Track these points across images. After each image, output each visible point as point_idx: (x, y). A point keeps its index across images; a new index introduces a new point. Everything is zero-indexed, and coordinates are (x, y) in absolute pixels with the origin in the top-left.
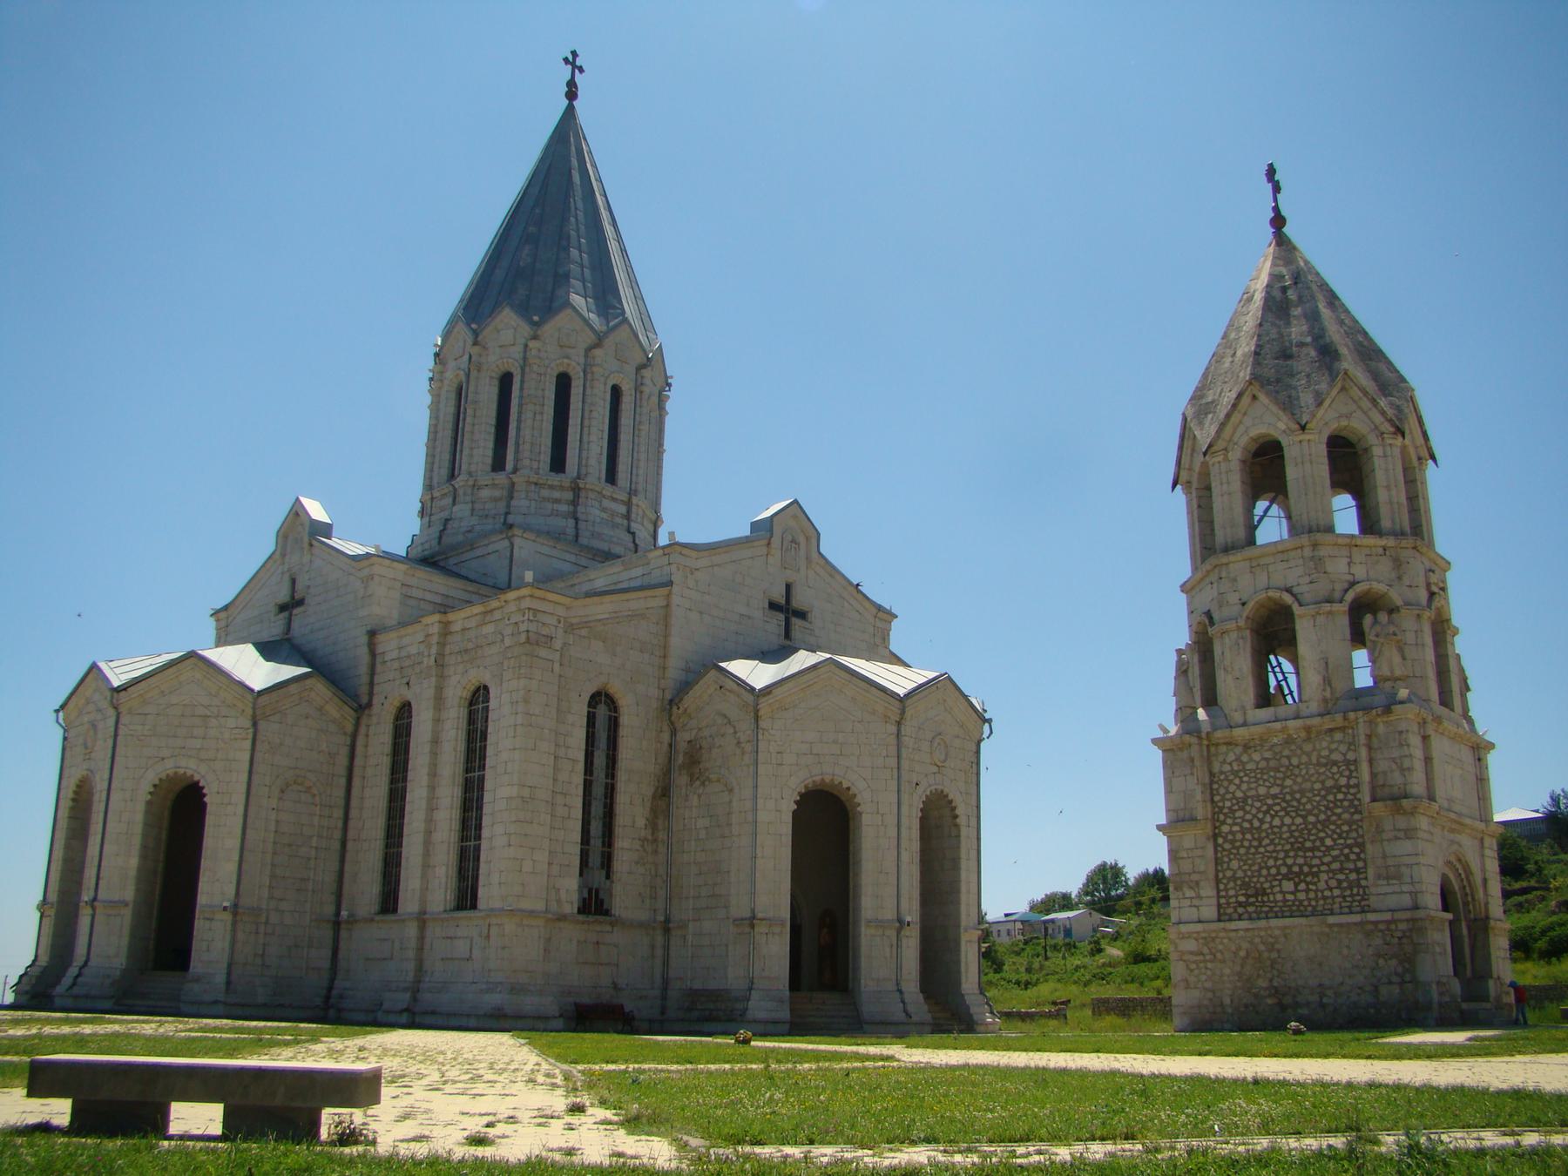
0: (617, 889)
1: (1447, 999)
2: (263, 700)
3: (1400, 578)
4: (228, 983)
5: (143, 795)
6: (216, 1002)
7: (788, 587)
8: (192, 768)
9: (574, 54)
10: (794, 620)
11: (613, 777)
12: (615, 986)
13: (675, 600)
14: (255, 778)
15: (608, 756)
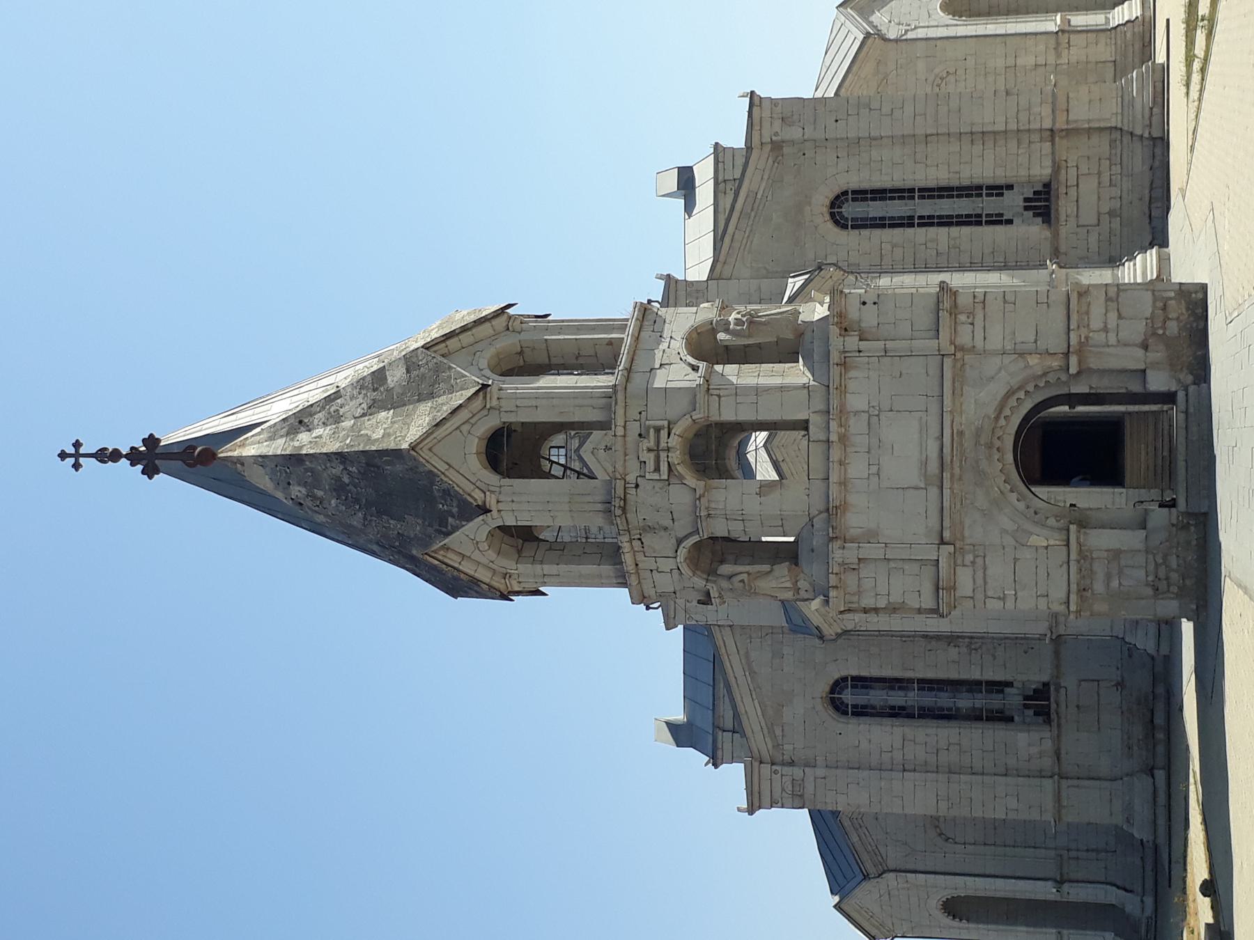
0: (1020, 678)
1: (1173, 562)
2: (872, 871)
3: (666, 529)
4: (1126, 890)
5: (964, 924)
6: (1142, 901)
8: (934, 903)
11: (910, 681)
12: (1120, 685)
14: (938, 869)
15: (892, 688)
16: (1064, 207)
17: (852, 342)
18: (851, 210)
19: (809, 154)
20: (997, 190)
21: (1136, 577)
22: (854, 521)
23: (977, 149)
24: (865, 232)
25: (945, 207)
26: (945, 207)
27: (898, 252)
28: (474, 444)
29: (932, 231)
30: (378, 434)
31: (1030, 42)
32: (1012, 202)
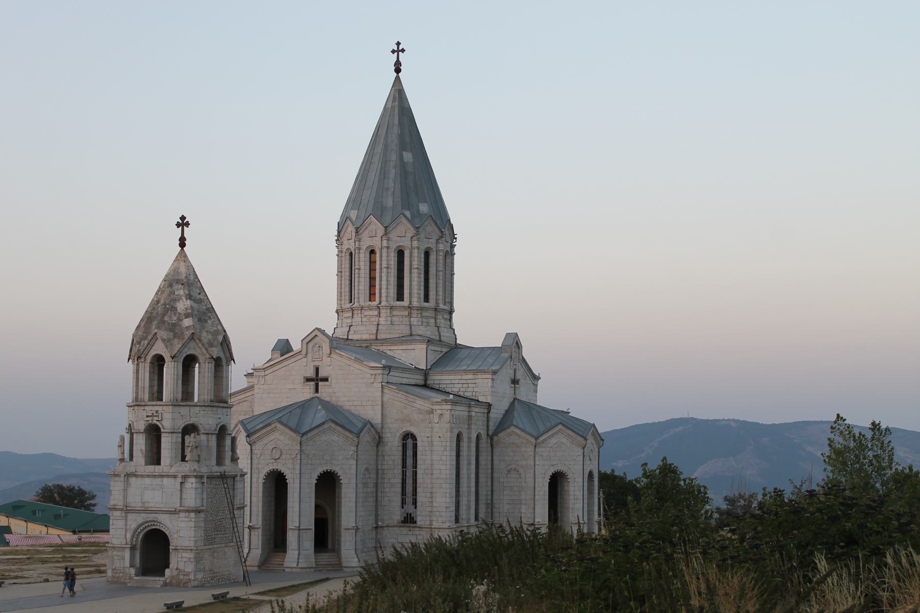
7: (317, 369)
9: (398, 44)
10: (320, 383)
13: (256, 391)
16: (405, 530)
17: (179, 480)
18: (410, 442)
19: (430, 425)
20: (415, 503)
21: (118, 564)
22: (133, 480)
23: (429, 495)
24: (400, 449)
25: (409, 481)
26: (409, 481)
27: (391, 462)
28: (158, 352)
29: (400, 476)
30: (166, 318)
31: (531, 510)
32: (410, 508)
